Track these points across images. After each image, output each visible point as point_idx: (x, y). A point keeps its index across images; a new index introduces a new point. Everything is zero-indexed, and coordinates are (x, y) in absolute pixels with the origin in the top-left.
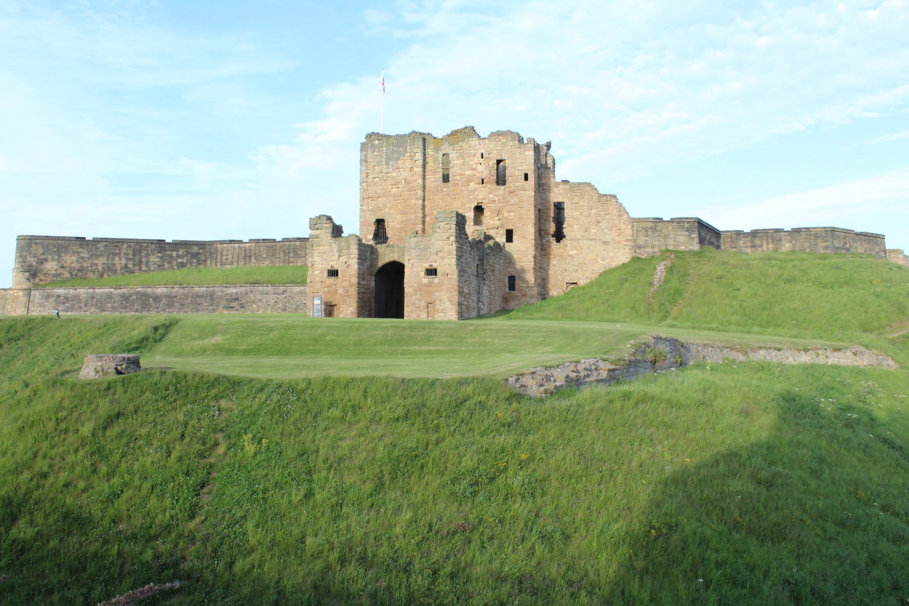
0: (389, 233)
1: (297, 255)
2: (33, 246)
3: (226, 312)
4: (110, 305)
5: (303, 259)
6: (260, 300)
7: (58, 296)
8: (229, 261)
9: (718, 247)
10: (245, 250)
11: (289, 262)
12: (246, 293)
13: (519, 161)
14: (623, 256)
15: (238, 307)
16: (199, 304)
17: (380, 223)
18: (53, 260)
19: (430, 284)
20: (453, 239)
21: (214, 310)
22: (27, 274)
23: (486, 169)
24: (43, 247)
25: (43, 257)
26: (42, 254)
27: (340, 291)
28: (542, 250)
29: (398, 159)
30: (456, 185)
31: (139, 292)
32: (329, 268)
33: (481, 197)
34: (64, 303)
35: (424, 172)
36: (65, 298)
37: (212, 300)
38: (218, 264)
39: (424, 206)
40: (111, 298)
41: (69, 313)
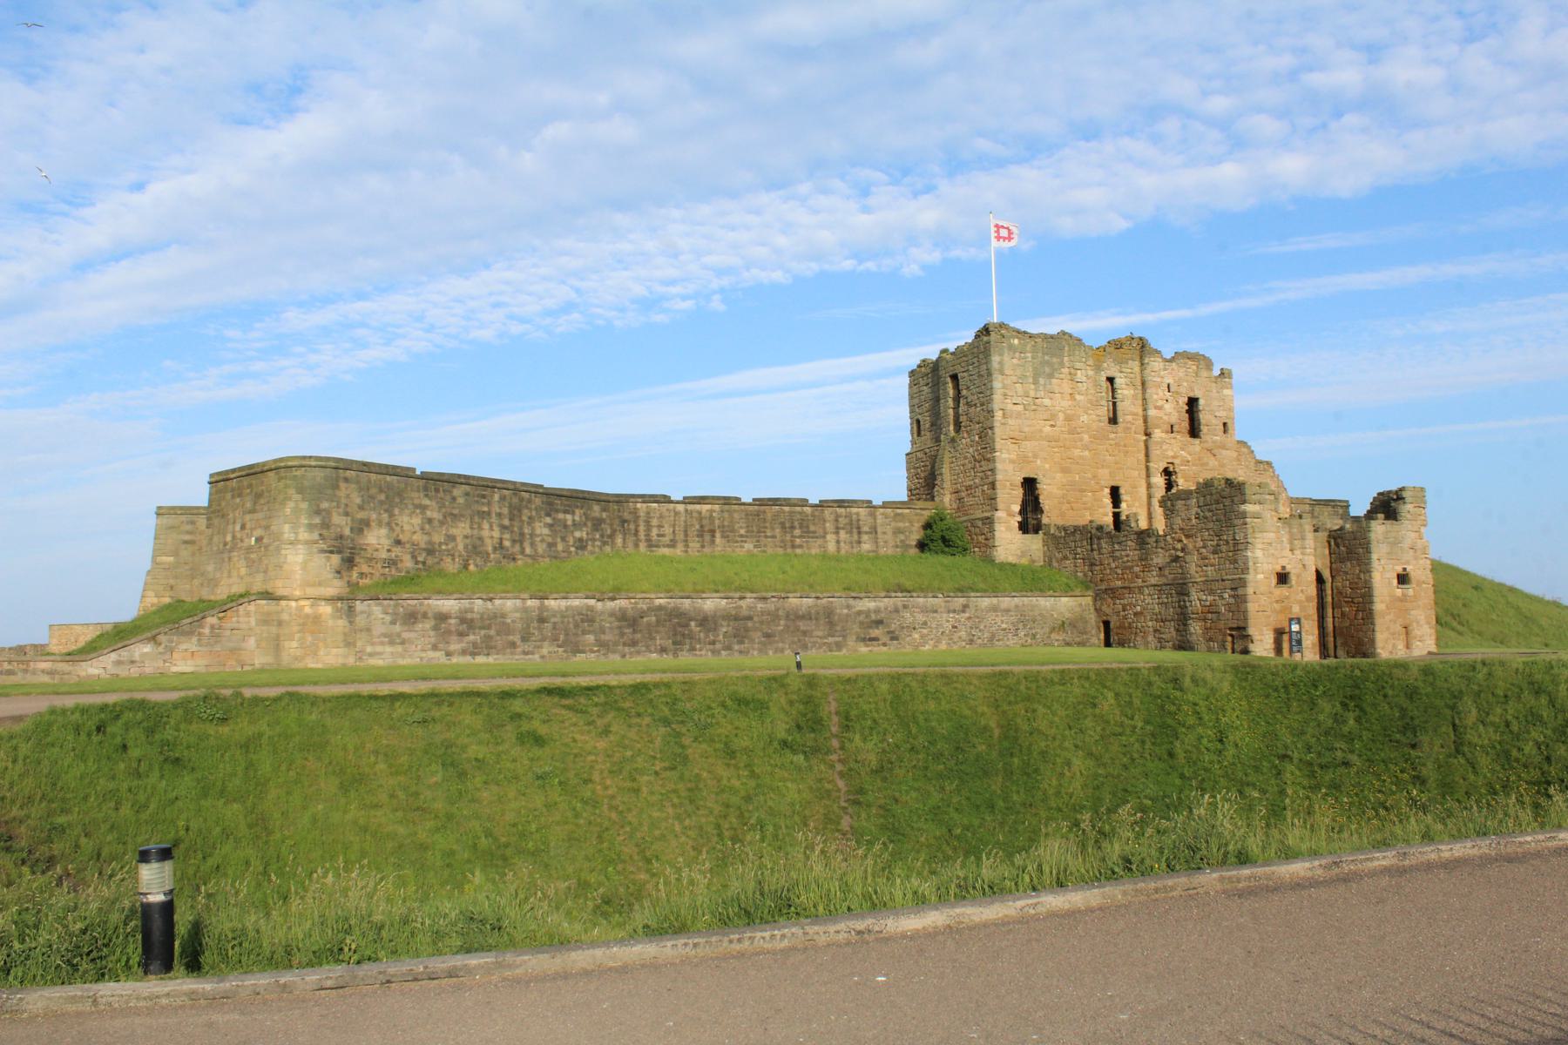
0: (1045, 502)
1: (807, 533)
2: (343, 485)
3: (863, 649)
4: (591, 638)
5: (820, 541)
6: (925, 623)
7: (442, 617)
8: (666, 540)
10: (701, 519)
11: (793, 547)
12: (897, 611)
13: (1216, 403)
15: (885, 639)
16: (805, 633)
18: (380, 524)
19: (1404, 599)
21: (839, 646)
22: (336, 559)
24: (360, 489)
25: (361, 515)
26: (361, 508)
29: (1051, 376)
31: (660, 608)
32: (1279, 569)
33: (1170, 453)
34: (461, 634)
36: (463, 620)
37: (831, 624)
38: (643, 547)
40: (592, 621)
41: (480, 659)
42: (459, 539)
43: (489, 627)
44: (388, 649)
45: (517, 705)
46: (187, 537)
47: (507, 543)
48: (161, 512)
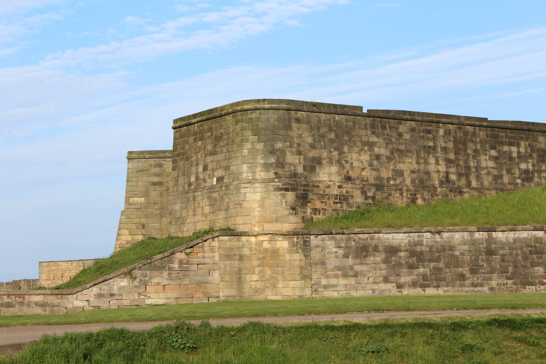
2: (294, 125)
7: (392, 250)
18: (331, 162)
22: (291, 196)
24: (311, 129)
25: (312, 154)
26: (313, 147)
34: (411, 267)
36: (412, 253)
41: (430, 291)
42: (406, 174)
43: (438, 260)
44: (342, 281)
45: (468, 338)
46: (156, 179)
47: (453, 177)
48: (131, 156)
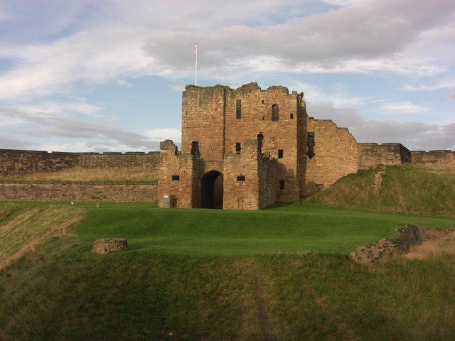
9: (410, 161)
14: (353, 169)
17: (195, 144)
20: (255, 157)
23: (265, 110)
27: (180, 190)
28: (301, 163)
30: (245, 120)
32: (173, 174)
35: (225, 111)
39: (224, 134)
